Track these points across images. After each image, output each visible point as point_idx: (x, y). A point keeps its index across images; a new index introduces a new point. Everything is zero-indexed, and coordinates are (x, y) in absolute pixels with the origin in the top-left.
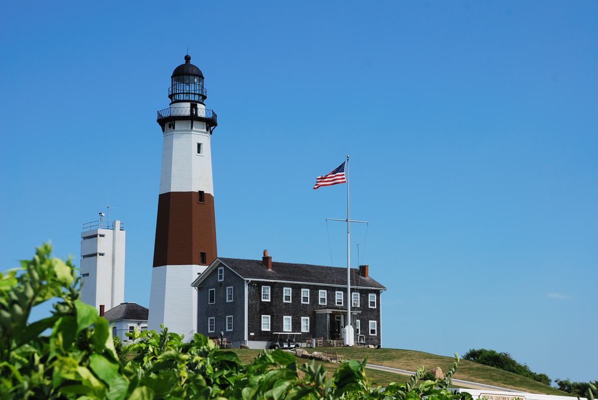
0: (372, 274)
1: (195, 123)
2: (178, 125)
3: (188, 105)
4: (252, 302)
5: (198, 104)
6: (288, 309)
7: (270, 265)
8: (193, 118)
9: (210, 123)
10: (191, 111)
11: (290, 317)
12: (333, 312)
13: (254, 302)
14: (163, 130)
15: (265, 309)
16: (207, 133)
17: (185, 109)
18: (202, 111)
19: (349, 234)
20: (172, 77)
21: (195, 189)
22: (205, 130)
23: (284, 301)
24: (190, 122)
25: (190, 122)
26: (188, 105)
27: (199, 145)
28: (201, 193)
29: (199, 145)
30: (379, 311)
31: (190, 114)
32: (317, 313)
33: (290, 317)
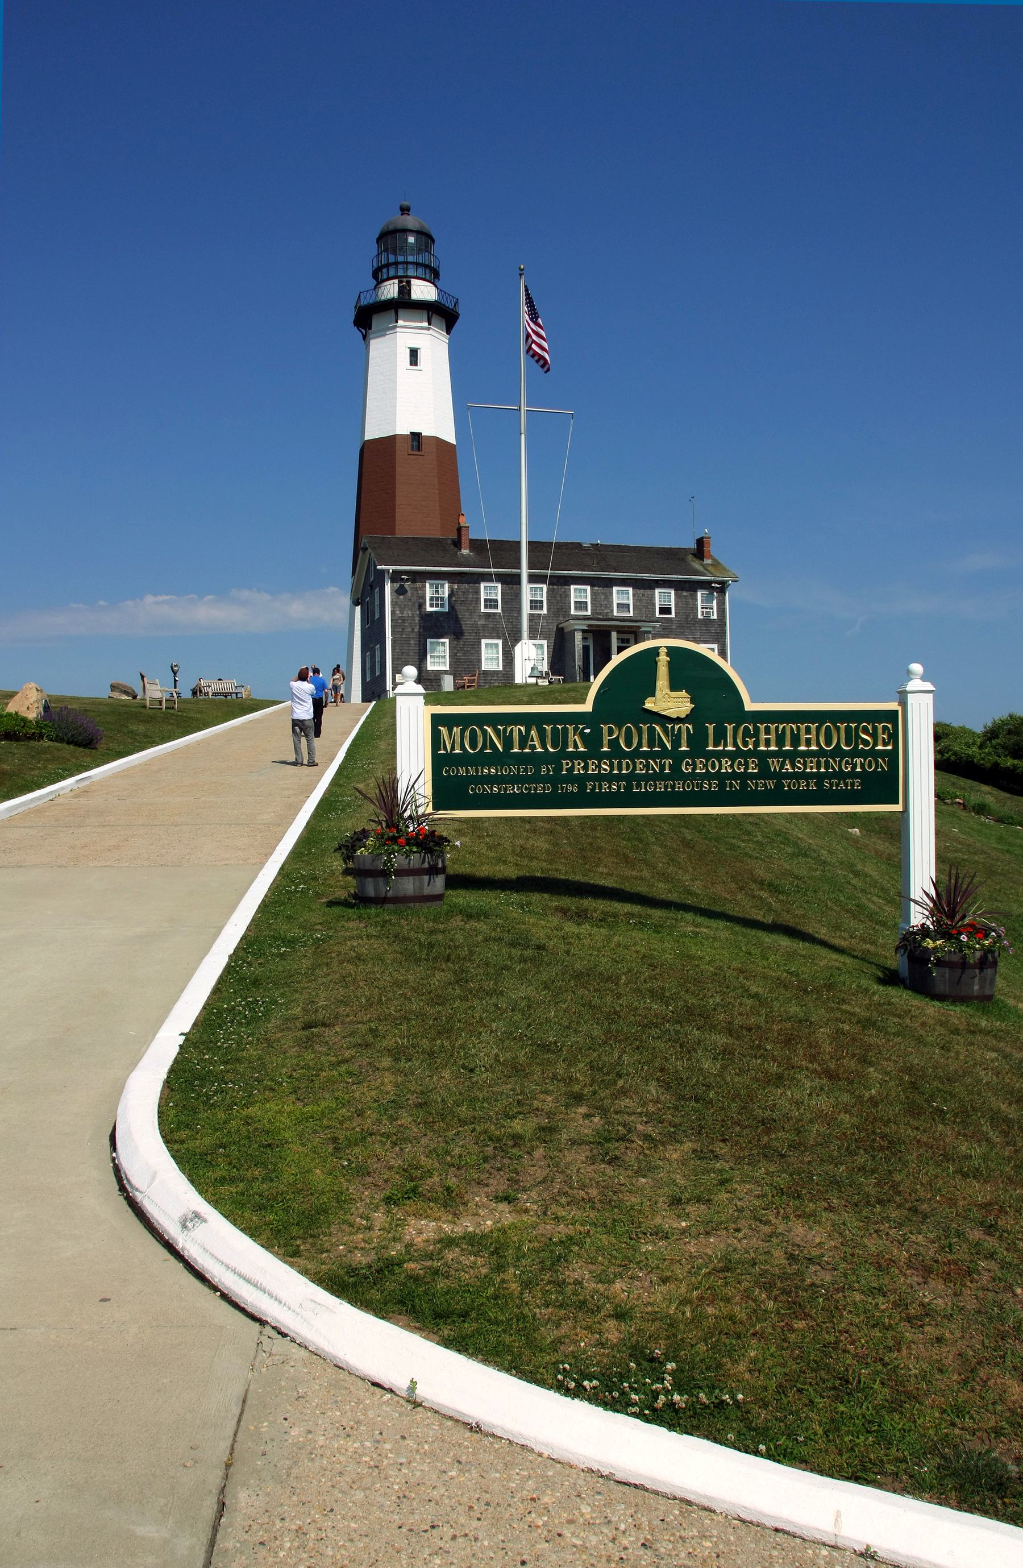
0: (714, 549)
1: (401, 312)
2: (377, 322)
3: (396, 281)
4: (402, 612)
5: (414, 282)
6: (492, 627)
7: (465, 541)
8: (404, 304)
9: (442, 314)
10: (400, 292)
11: (500, 642)
12: (589, 626)
13: (408, 613)
14: (364, 337)
15: (434, 626)
16: (428, 329)
17: (390, 290)
18: (423, 291)
19: (523, 436)
20: (379, 240)
21: (403, 428)
22: (426, 324)
23: (483, 610)
24: (393, 311)
25: (393, 311)
26: (396, 281)
27: (414, 353)
28: (416, 436)
29: (414, 353)
30: (724, 624)
31: (396, 296)
32: (566, 631)
33: (500, 642)
